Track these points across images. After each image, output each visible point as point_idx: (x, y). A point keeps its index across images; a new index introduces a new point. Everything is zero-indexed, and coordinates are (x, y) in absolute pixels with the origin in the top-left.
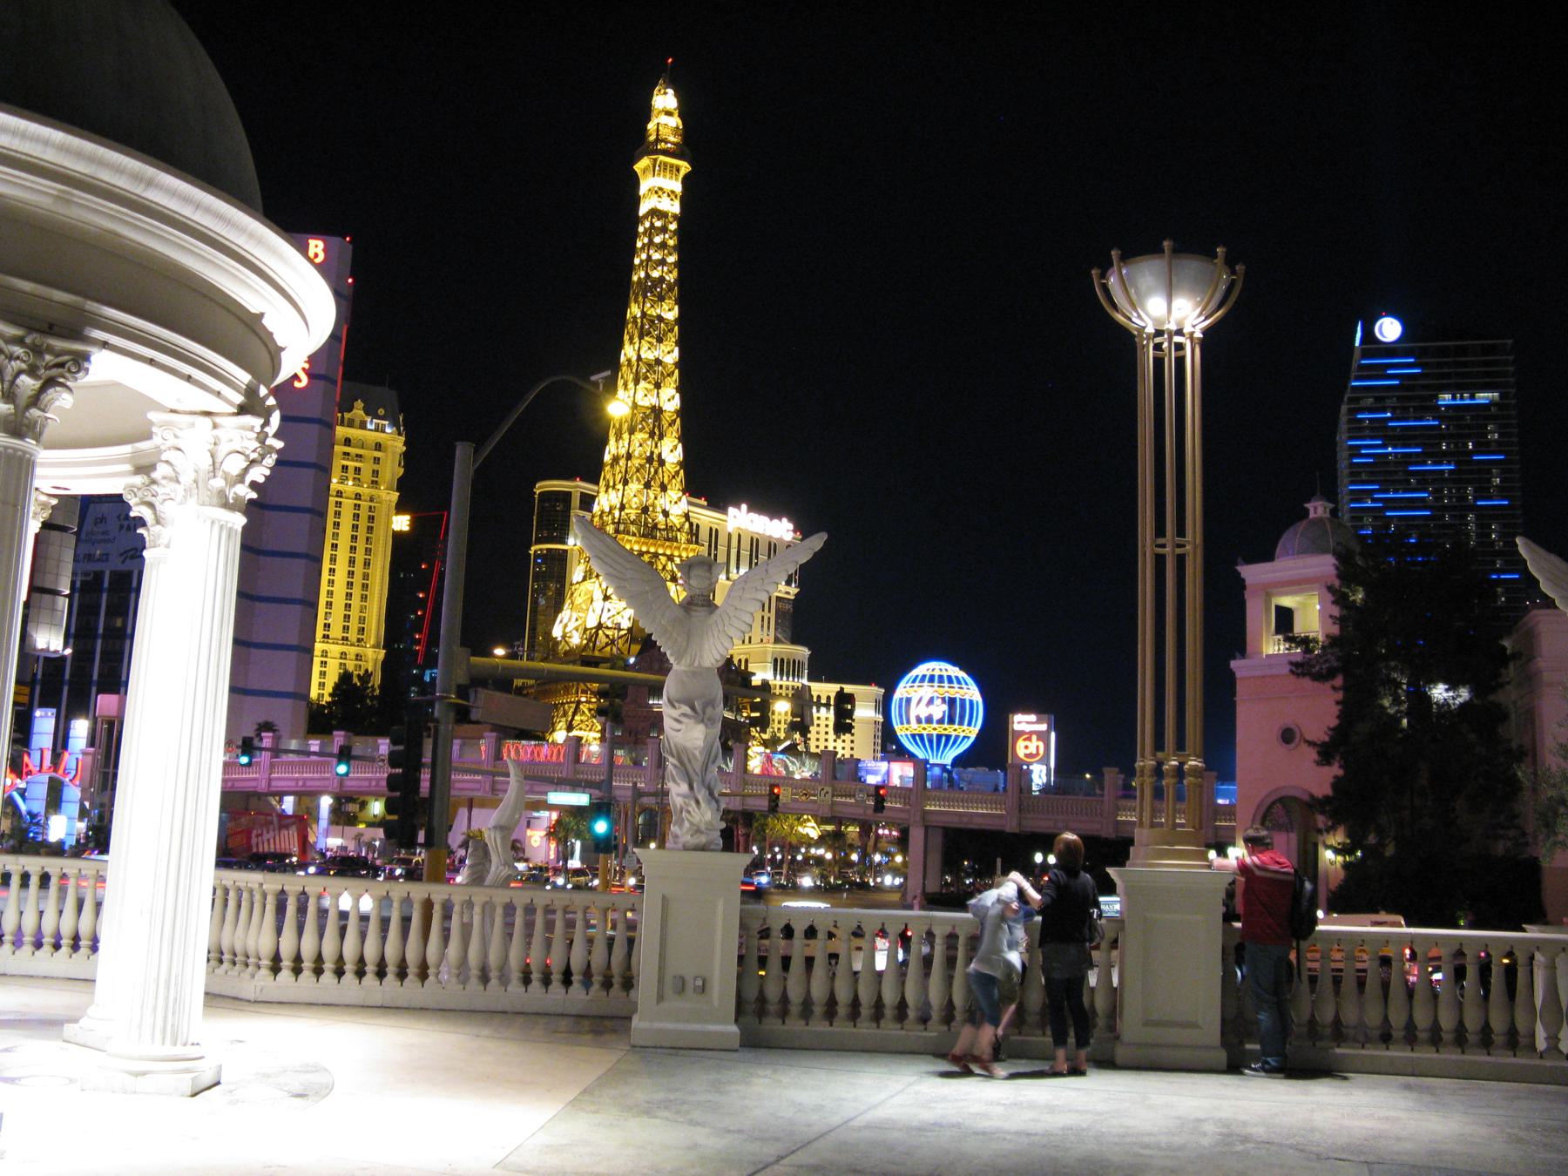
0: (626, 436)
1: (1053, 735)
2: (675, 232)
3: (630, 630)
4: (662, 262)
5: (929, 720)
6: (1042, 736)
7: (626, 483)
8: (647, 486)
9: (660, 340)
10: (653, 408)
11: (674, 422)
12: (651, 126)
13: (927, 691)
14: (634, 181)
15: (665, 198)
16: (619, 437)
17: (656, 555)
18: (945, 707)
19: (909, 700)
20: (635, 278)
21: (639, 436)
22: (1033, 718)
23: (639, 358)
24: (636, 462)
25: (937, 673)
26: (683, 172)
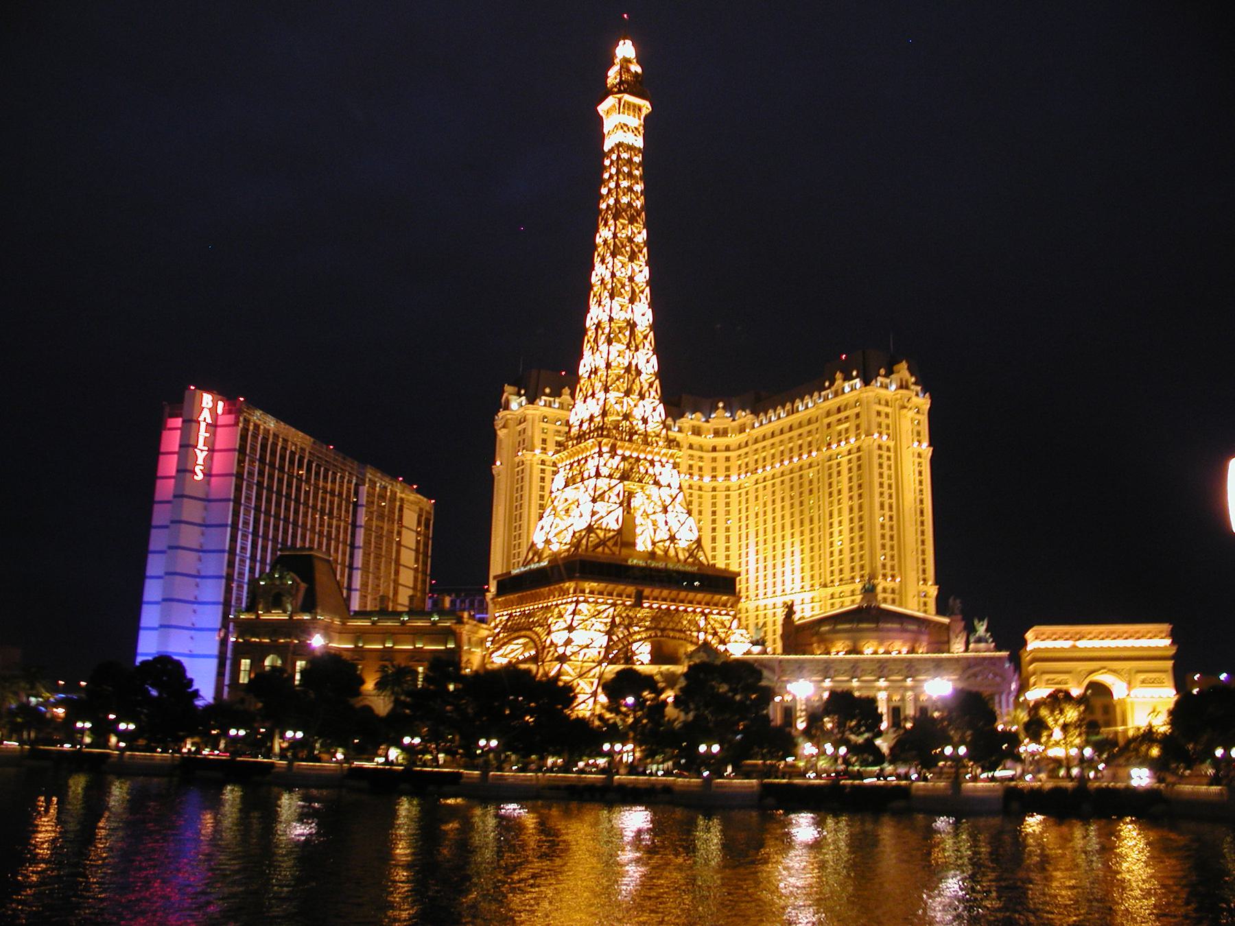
0: (604, 347)
2: (640, 164)
3: (619, 531)
4: (630, 189)
7: (606, 390)
8: (628, 393)
9: (631, 259)
10: (628, 322)
11: (646, 337)
14: (600, 121)
15: (630, 134)
17: (638, 459)
20: (603, 206)
21: (617, 347)
23: (613, 275)
24: (614, 372)
26: (645, 112)
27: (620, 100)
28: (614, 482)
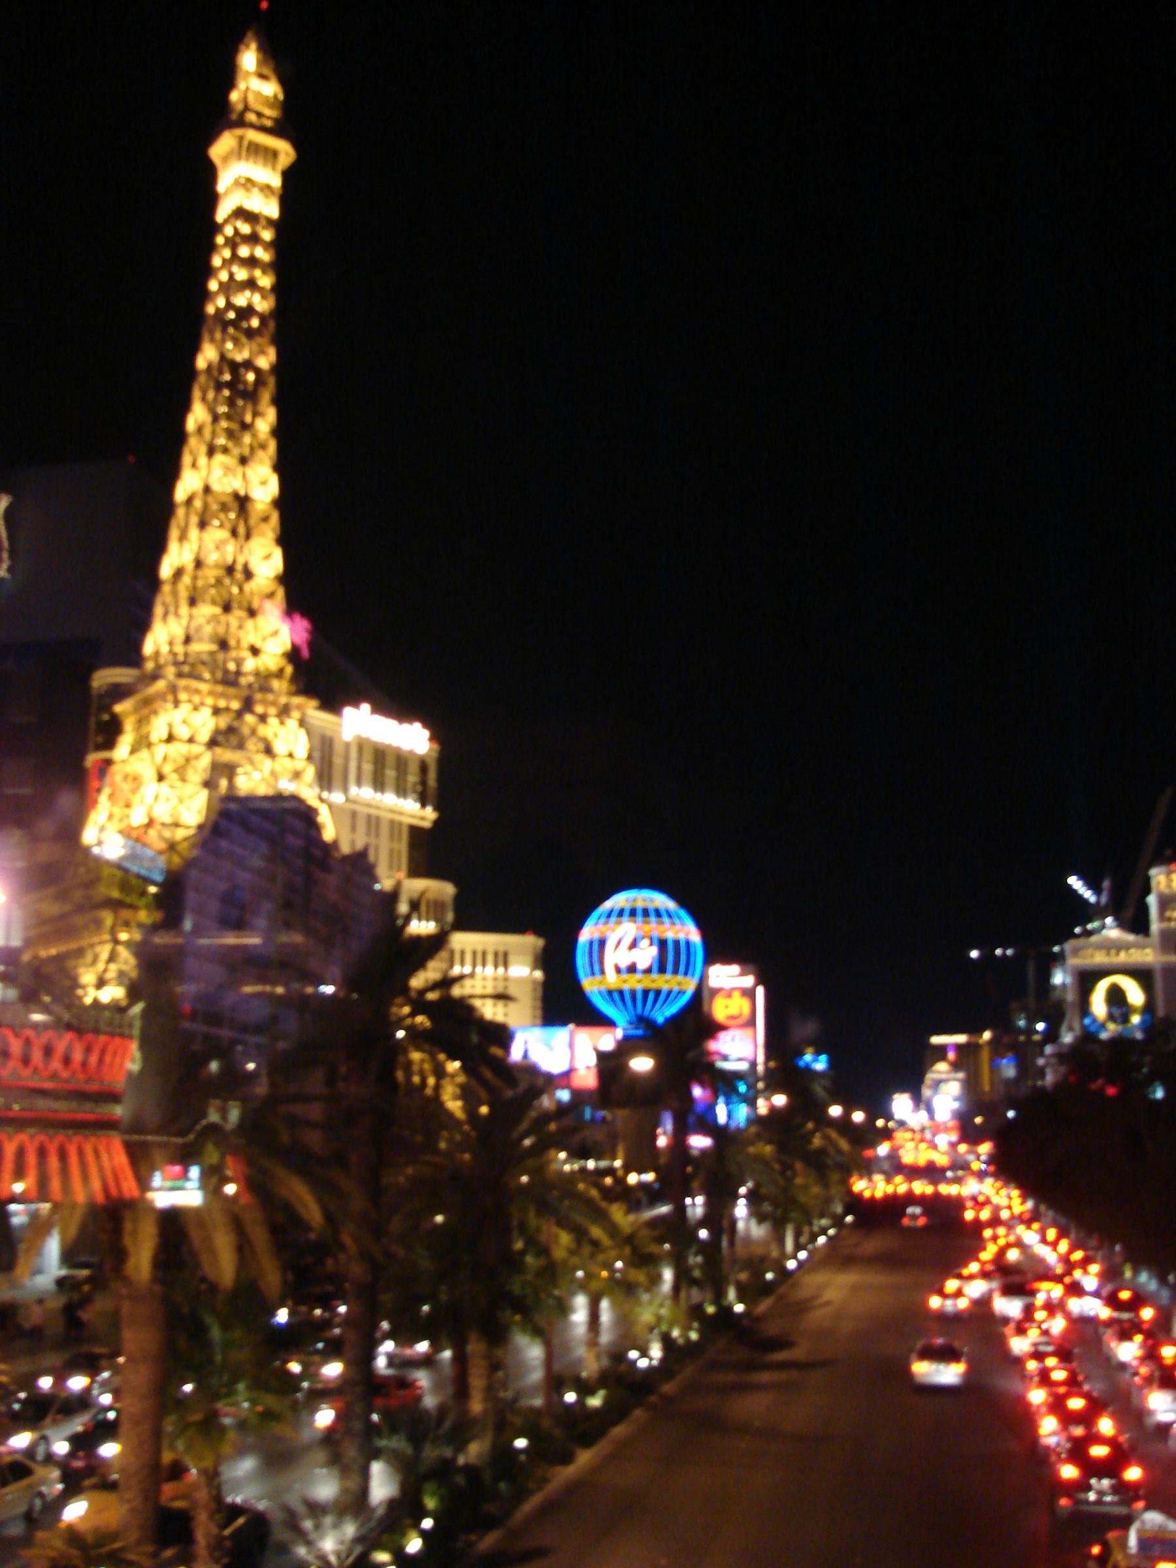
1: (760, 991)
5: (632, 969)
6: (749, 994)
12: (234, 96)
13: (628, 929)
14: (209, 172)
16: (183, 537)
18: (654, 951)
19: (602, 943)
21: (216, 533)
22: (735, 969)
25: (640, 905)
27: (241, 138)
28: (196, 749)
